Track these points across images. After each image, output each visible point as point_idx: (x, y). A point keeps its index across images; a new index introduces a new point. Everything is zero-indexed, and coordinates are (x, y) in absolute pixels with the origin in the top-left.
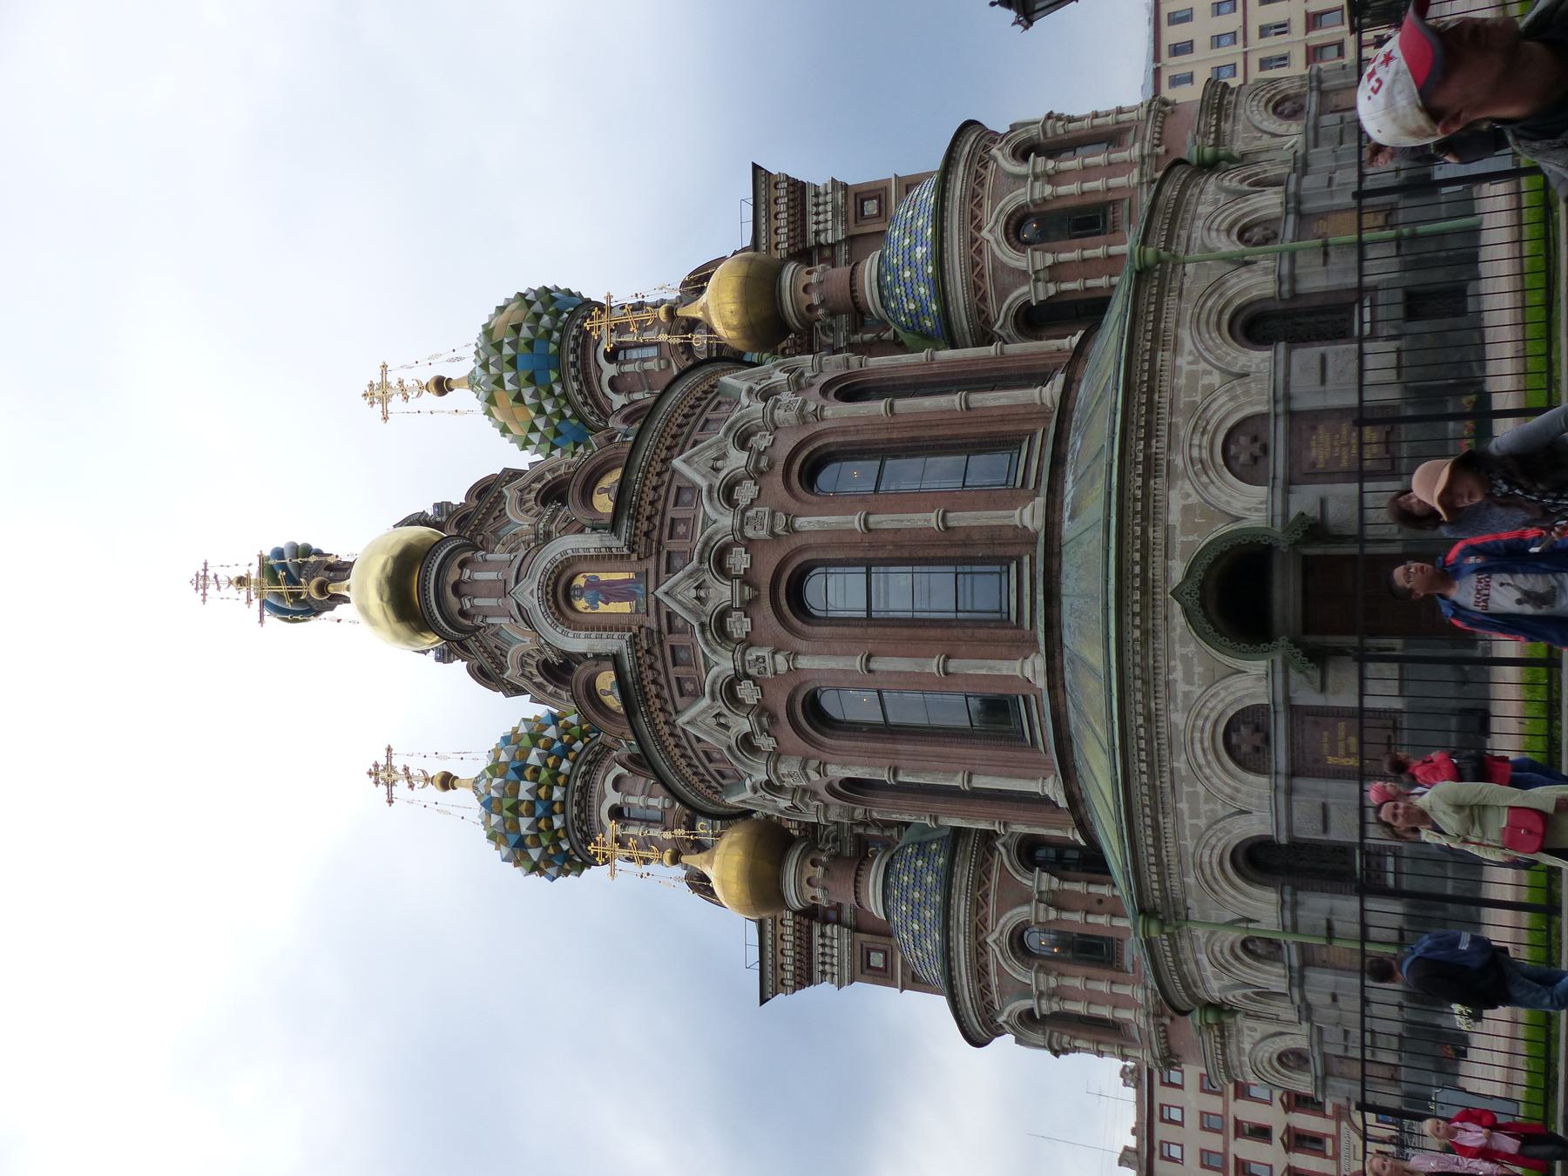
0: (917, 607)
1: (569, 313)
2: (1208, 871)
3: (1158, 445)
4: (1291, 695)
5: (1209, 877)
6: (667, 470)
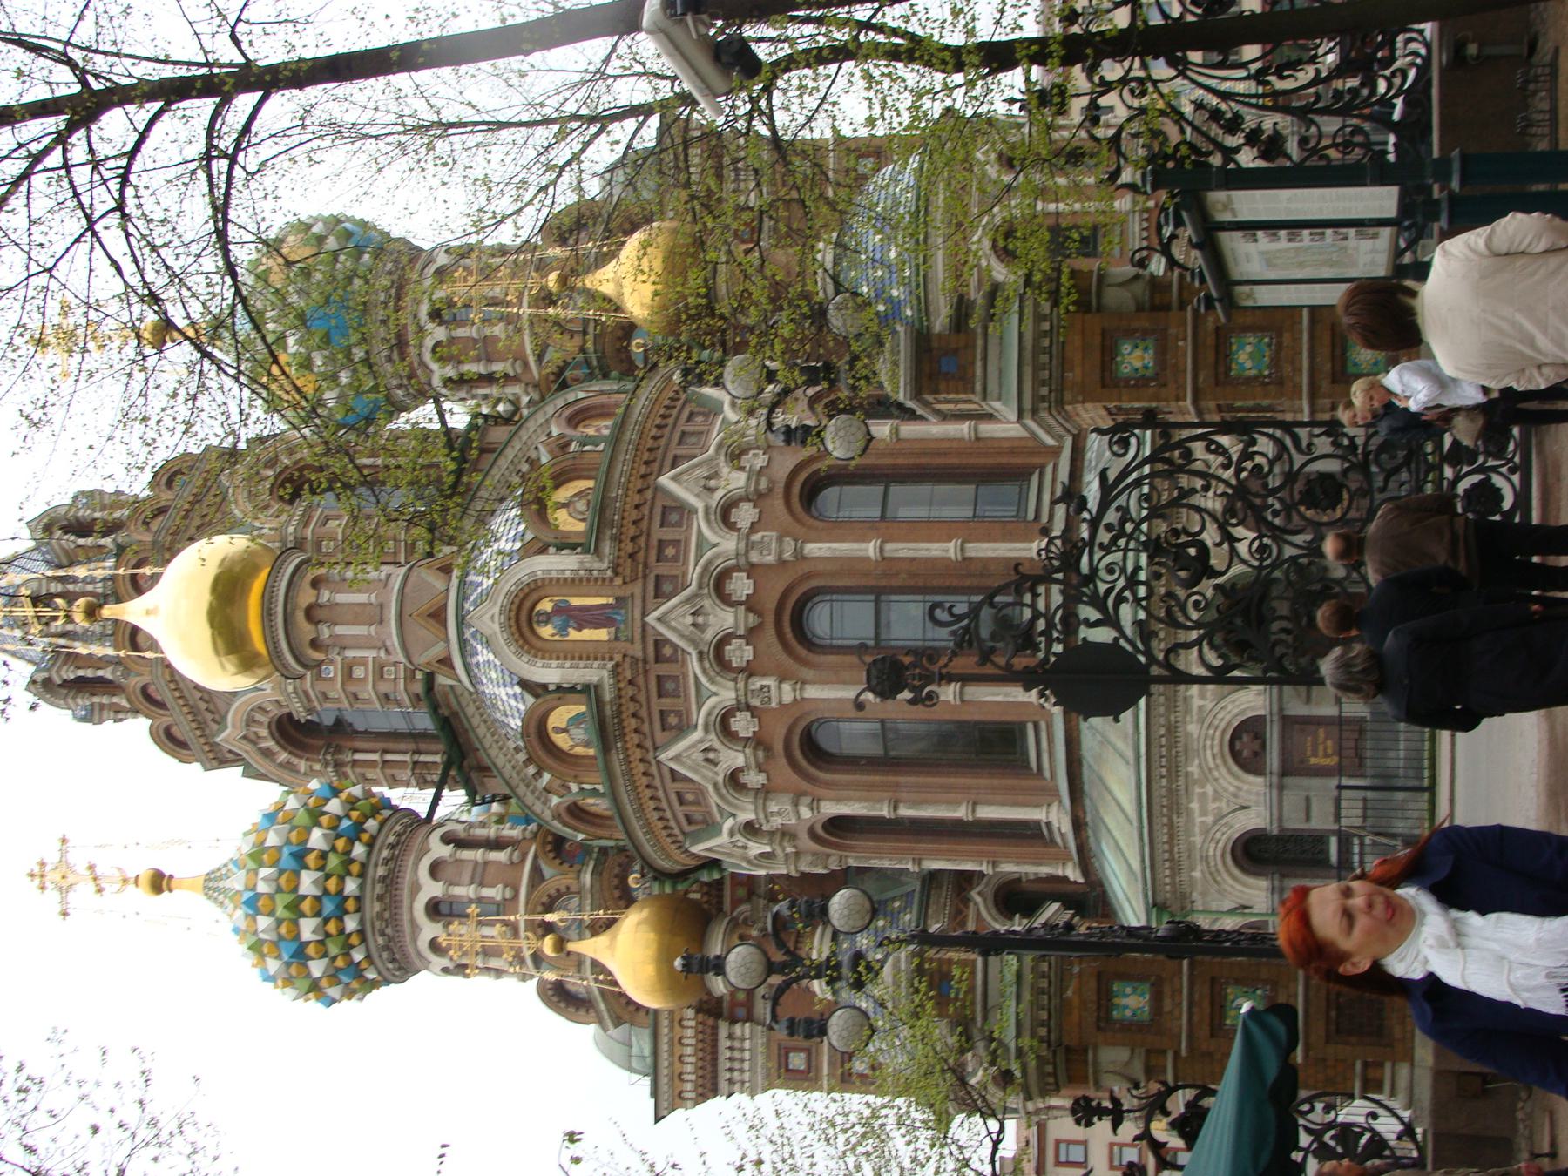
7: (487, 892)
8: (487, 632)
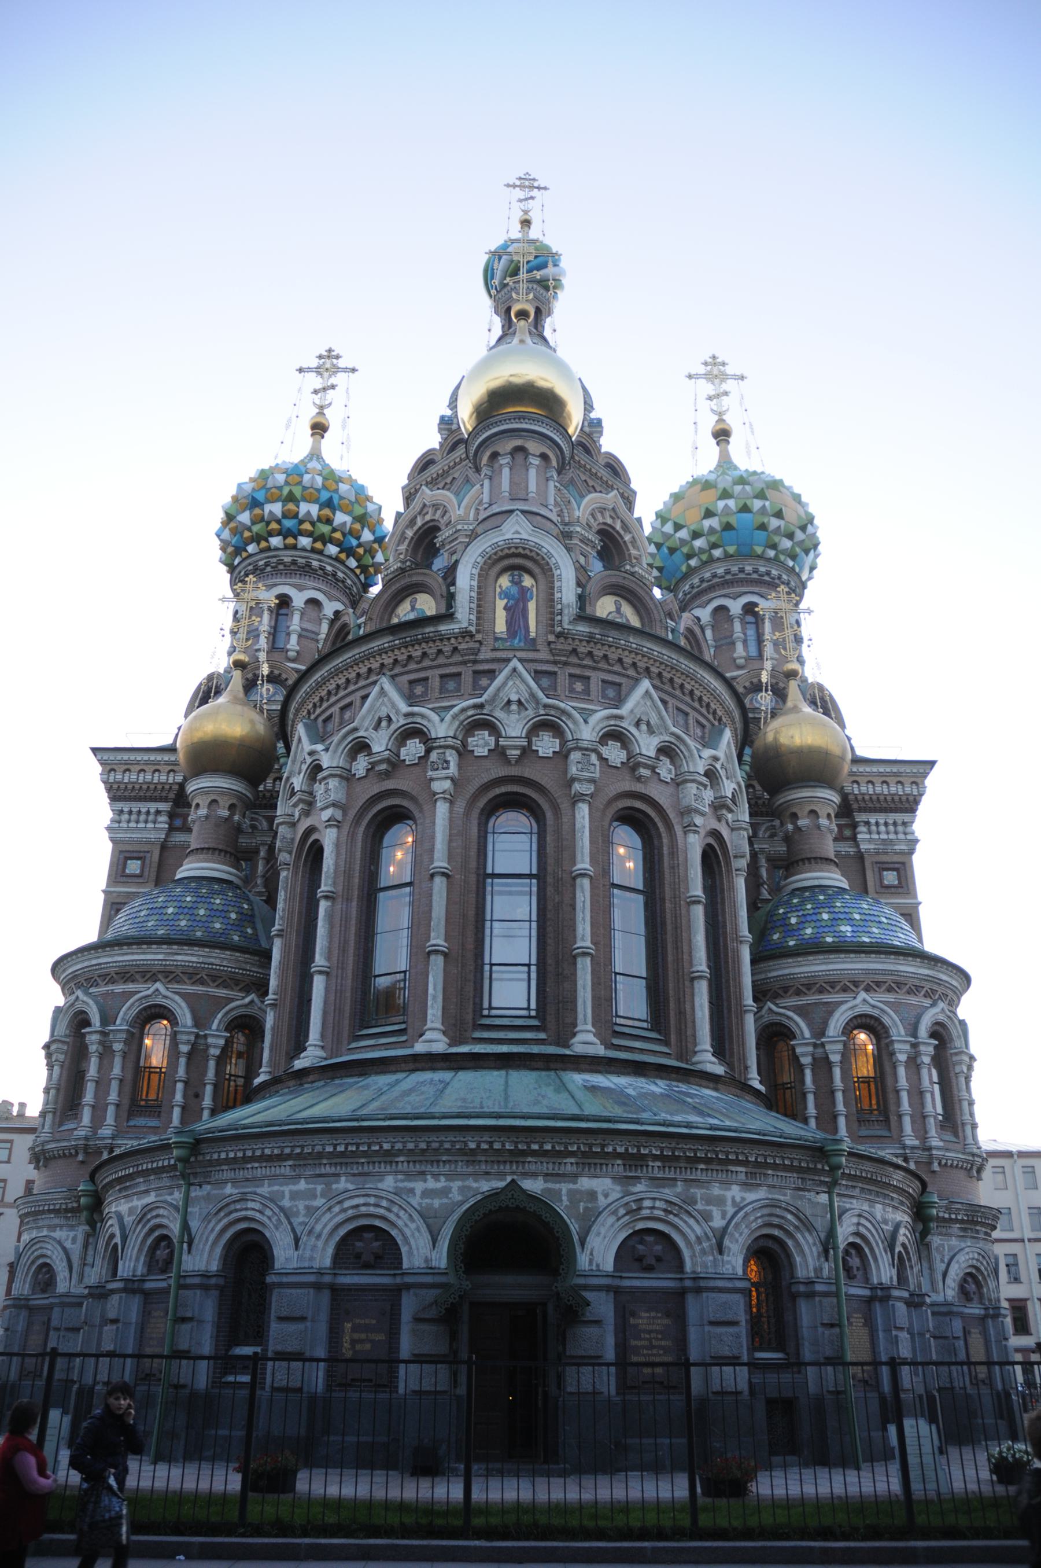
0: (496, 925)
1: (793, 568)
2: (238, 1207)
3: (656, 1169)
4: (412, 1291)
5: (232, 1207)
6: (638, 673)
7: (294, 638)
8: (505, 527)
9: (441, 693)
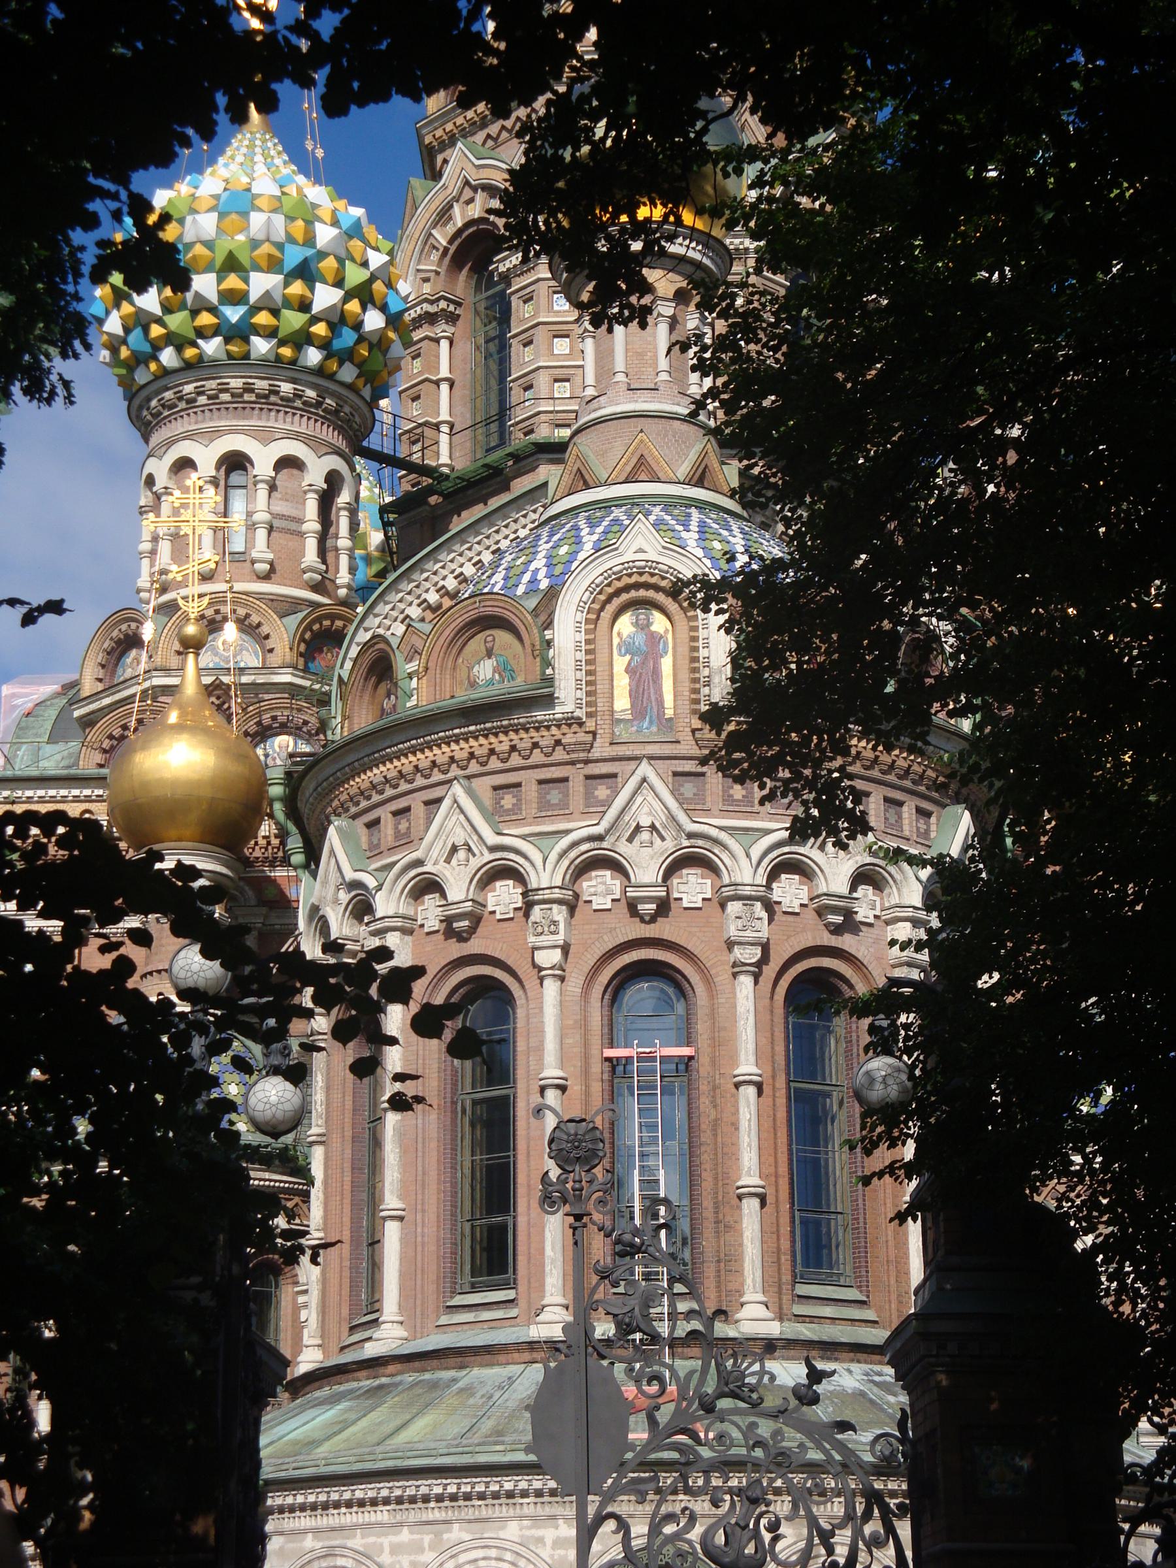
9: (540, 810)
